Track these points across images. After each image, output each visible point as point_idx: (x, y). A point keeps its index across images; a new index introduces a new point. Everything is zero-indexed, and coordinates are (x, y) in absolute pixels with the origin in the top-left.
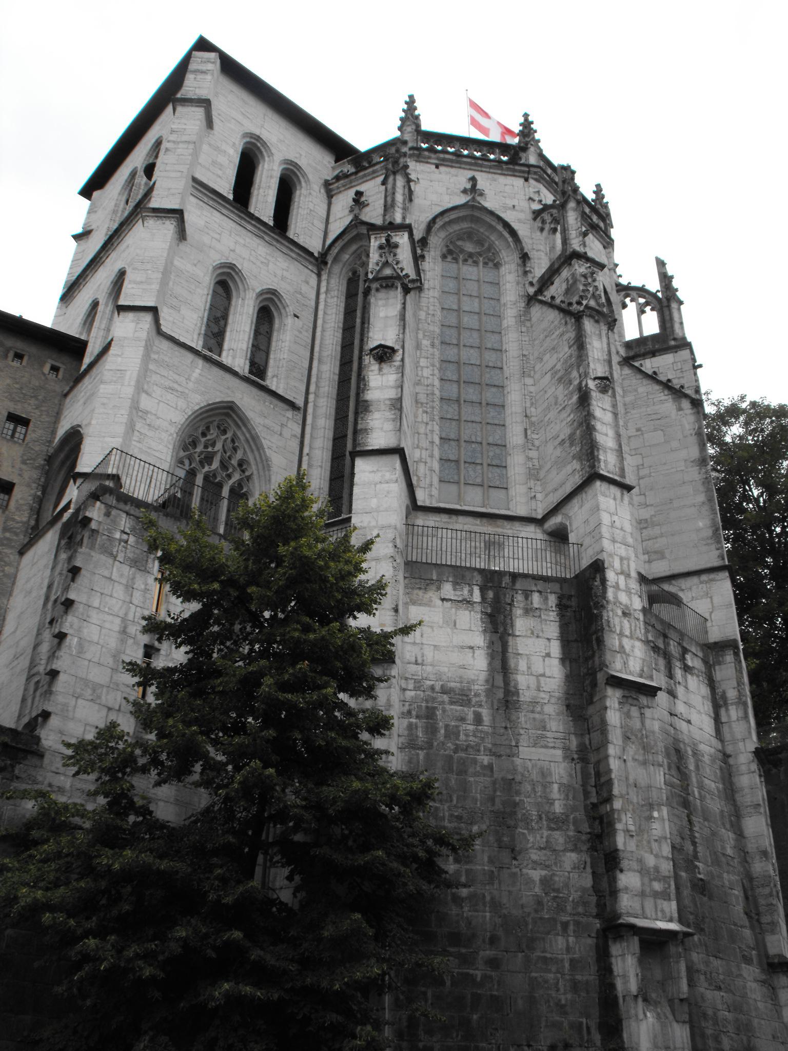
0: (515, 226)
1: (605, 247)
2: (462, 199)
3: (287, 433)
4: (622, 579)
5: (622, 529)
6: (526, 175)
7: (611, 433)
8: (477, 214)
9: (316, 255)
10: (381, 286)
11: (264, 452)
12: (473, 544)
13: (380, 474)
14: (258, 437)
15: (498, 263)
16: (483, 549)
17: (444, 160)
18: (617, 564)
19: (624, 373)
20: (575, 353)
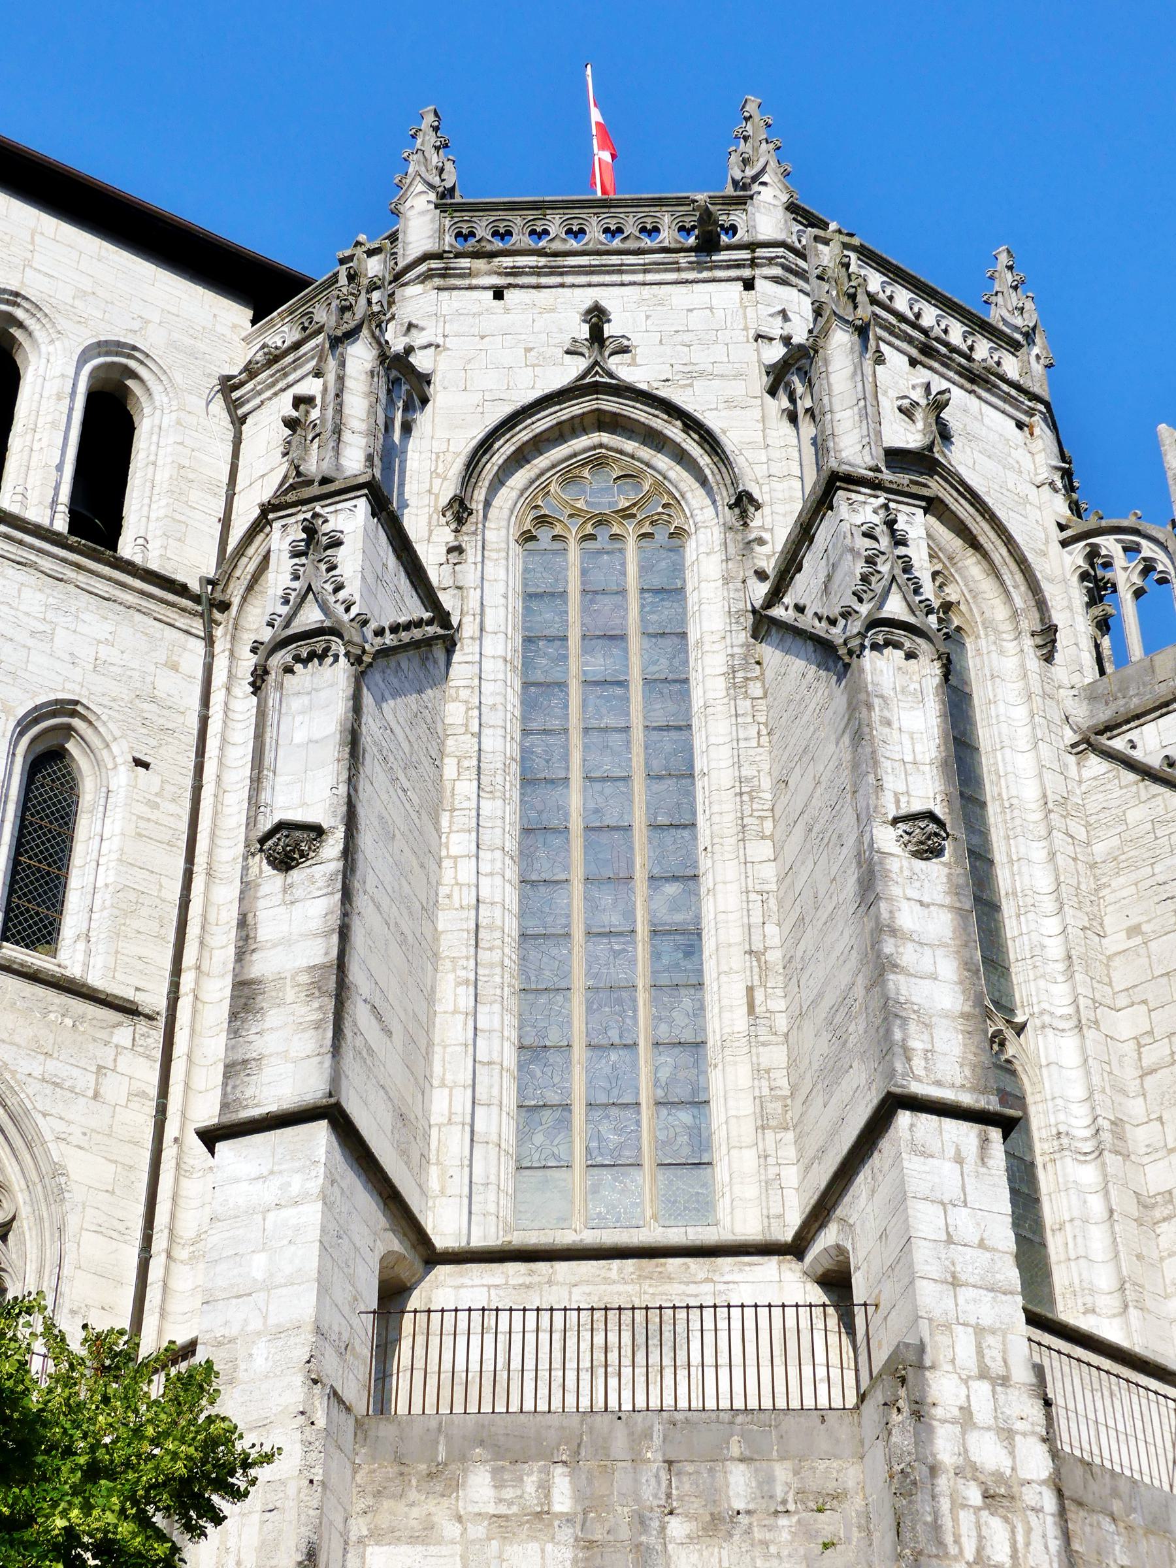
0: (712, 421)
1: (1020, 425)
2: (570, 370)
3: (115, 1089)
4: (982, 1389)
5: (982, 1245)
6: (746, 273)
8: (610, 404)
9: (195, 586)
11: (47, 1152)
12: (599, 1339)
13: (275, 1183)
14: (27, 1112)
16: (627, 1350)
17: (515, 272)
18: (964, 1346)
19: (1087, 773)
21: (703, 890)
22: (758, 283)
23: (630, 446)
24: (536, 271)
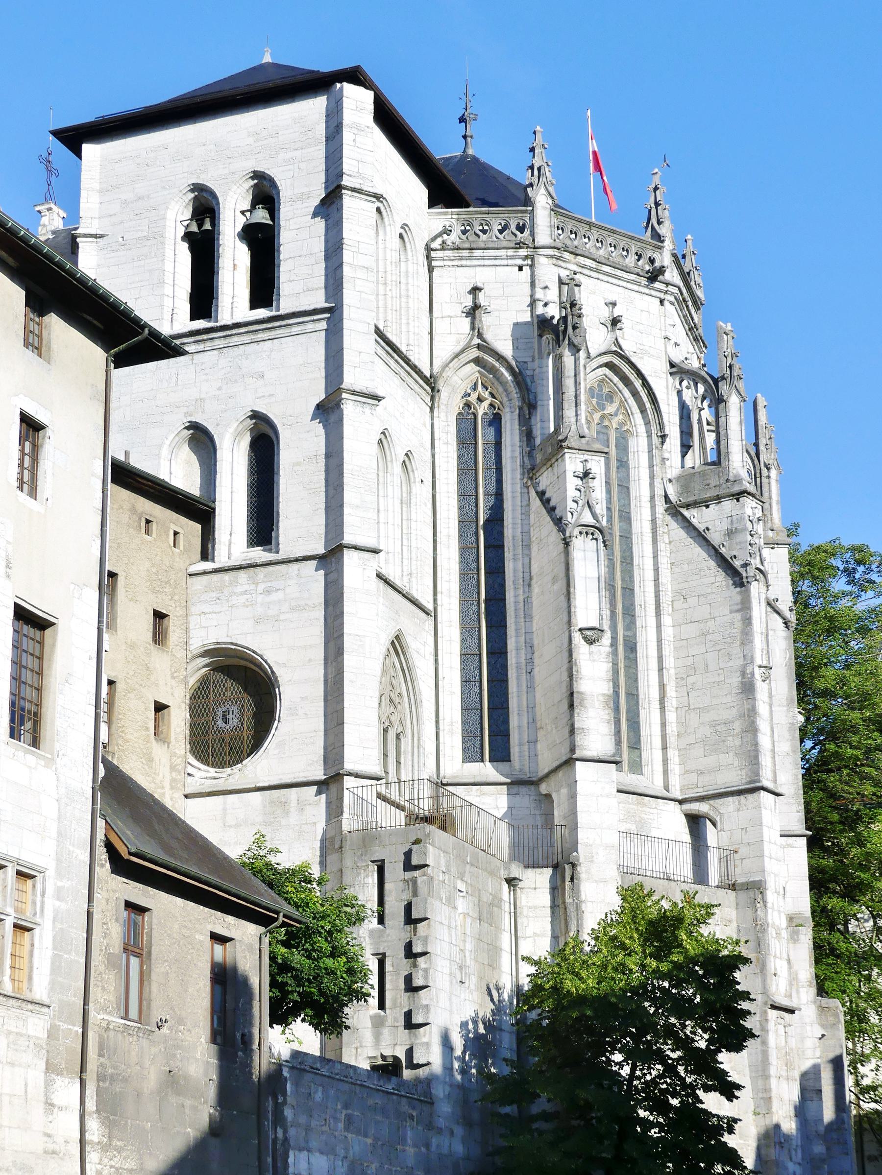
4: (775, 895)
6: (662, 296)
7: (769, 732)
10: (581, 533)
15: (628, 431)
20: (739, 625)
21: (638, 624)
22: (666, 303)
23: (616, 379)
24: (591, 269)
